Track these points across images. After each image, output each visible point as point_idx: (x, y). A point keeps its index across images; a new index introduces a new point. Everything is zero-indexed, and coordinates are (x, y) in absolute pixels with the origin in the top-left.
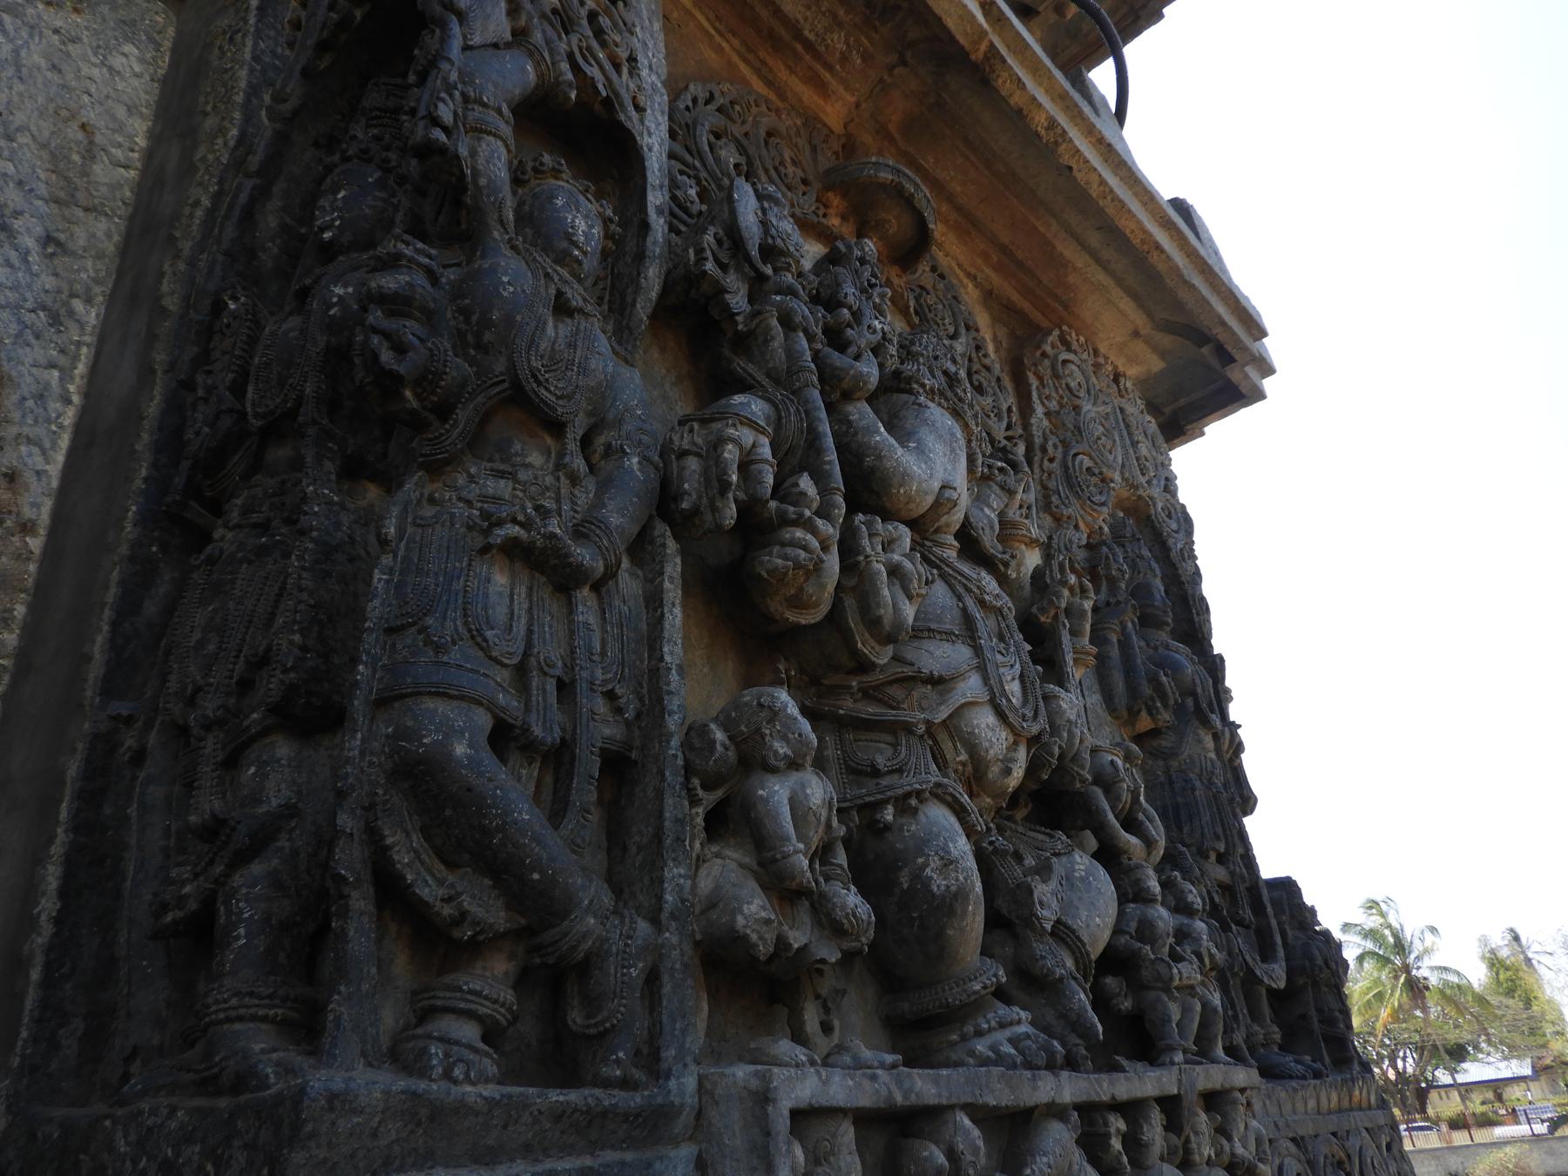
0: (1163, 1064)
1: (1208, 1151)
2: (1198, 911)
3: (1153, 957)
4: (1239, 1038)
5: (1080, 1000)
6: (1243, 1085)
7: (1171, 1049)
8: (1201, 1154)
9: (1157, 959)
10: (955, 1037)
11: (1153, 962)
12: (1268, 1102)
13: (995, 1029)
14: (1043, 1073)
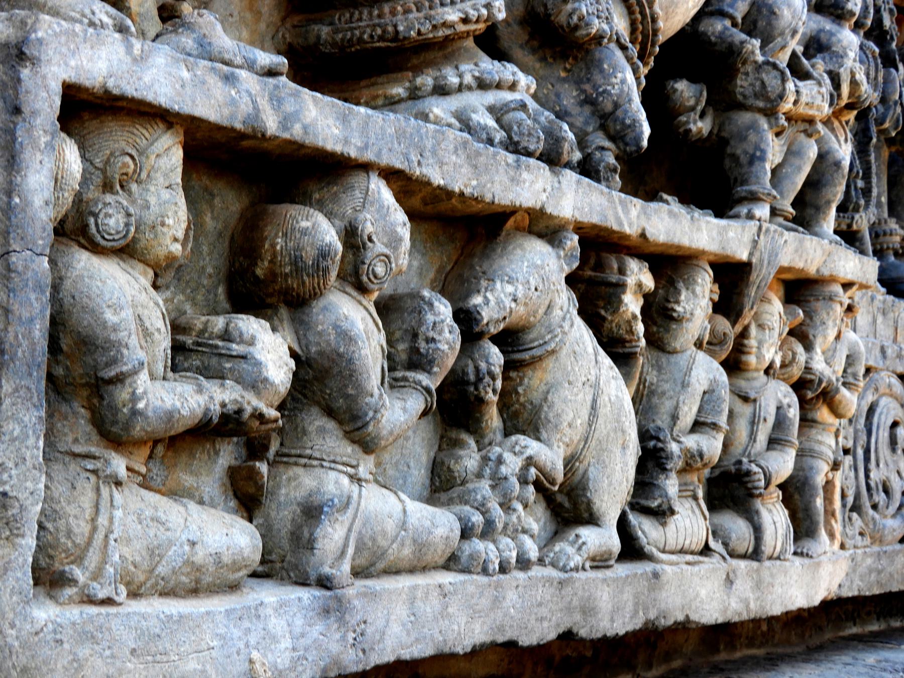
0: (736, 216)
1: (771, 354)
2: (852, 14)
3: (760, 58)
4: (863, 221)
5: (623, 81)
6: (850, 277)
7: (754, 198)
8: (760, 357)
9: (767, 63)
10: (399, 91)
11: (759, 67)
12: (880, 319)
13: (470, 88)
14: (532, 161)
